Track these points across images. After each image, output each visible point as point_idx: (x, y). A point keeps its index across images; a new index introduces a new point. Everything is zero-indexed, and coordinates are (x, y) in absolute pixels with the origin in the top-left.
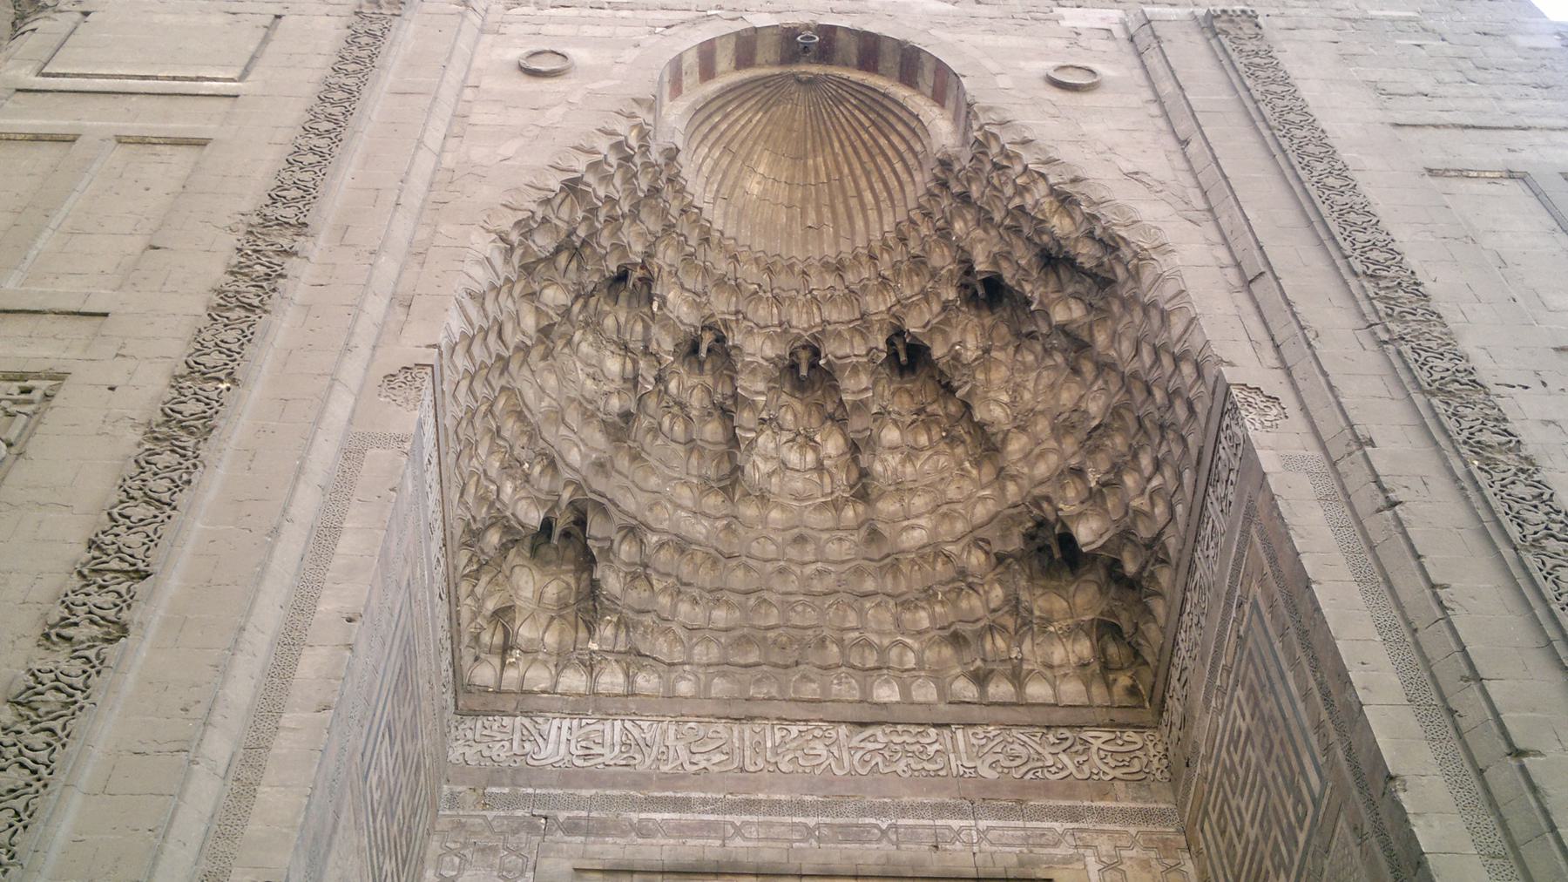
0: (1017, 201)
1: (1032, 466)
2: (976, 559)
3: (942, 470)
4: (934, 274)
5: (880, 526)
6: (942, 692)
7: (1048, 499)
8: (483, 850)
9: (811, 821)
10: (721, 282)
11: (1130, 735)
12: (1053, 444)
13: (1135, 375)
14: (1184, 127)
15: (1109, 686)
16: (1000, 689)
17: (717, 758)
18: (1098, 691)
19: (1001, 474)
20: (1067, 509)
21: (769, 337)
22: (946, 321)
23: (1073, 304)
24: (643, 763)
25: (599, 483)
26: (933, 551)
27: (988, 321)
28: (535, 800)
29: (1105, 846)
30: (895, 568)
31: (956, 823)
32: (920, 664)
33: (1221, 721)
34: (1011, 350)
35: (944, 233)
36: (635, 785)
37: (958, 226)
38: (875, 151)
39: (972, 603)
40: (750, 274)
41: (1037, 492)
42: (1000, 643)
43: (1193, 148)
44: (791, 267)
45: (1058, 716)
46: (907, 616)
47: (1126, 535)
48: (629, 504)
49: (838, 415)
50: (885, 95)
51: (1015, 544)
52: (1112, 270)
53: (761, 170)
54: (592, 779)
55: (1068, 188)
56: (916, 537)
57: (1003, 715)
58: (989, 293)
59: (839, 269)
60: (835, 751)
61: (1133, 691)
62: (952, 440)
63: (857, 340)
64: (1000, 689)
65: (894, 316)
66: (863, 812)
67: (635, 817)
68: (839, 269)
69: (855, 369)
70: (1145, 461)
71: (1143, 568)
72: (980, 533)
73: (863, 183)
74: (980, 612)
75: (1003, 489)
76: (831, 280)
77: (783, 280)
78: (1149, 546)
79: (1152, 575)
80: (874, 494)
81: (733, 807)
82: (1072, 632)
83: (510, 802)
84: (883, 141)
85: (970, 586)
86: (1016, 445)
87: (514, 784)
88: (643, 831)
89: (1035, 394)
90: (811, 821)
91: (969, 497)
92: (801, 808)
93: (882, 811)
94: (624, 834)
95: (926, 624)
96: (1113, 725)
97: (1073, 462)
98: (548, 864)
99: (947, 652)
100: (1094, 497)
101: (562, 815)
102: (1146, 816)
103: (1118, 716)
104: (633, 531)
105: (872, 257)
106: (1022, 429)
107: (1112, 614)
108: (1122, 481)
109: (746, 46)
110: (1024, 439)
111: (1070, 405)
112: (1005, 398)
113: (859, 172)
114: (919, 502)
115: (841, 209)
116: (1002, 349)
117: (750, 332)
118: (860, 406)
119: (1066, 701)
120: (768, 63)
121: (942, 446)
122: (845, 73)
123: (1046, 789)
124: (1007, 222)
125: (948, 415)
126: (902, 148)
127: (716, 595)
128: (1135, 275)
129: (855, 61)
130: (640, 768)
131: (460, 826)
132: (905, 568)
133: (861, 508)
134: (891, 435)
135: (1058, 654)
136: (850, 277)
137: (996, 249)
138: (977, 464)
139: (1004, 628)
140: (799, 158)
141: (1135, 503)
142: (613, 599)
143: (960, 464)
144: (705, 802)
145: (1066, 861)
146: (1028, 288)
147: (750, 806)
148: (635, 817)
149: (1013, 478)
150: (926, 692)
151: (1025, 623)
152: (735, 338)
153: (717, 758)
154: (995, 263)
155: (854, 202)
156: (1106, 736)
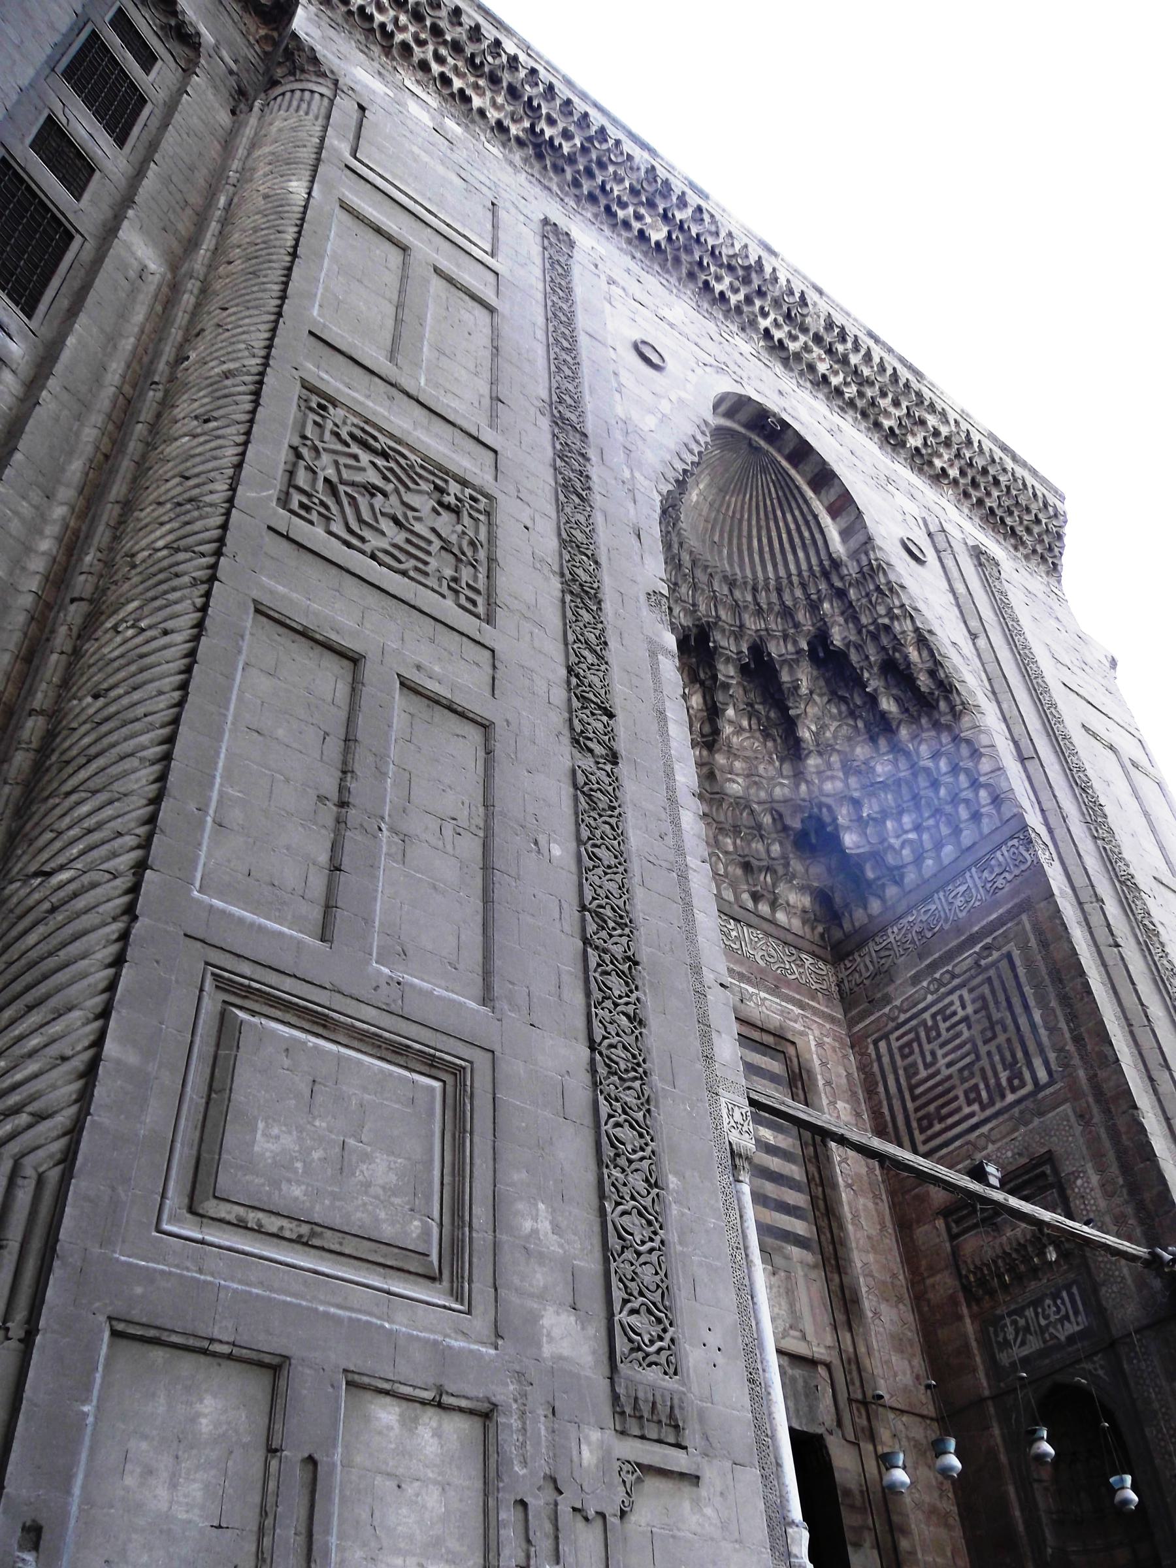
0: (886, 621)
1: (822, 781)
2: (767, 820)
3: (756, 751)
4: (797, 625)
5: (717, 773)
7: (829, 808)
11: (821, 964)
12: (841, 774)
13: (927, 770)
14: (974, 624)
15: (813, 929)
16: (764, 908)
18: (807, 929)
19: (798, 776)
20: (841, 820)
21: (684, 609)
22: (797, 661)
23: (892, 701)
26: (742, 804)
27: (815, 673)
29: (817, 1033)
30: (720, 802)
31: (751, 990)
33: (930, 998)
34: (825, 699)
35: (814, 607)
37: (826, 605)
38: (771, 516)
39: (757, 846)
41: (824, 799)
43: (982, 642)
44: (706, 567)
45: (790, 938)
46: (720, 838)
47: (876, 856)
49: (708, 683)
50: (797, 487)
51: (796, 824)
52: (938, 701)
53: (701, 486)
55: (927, 635)
56: (735, 788)
57: (765, 925)
58: (827, 658)
59: (732, 584)
61: (822, 935)
62: (766, 735)
63: (732, 640)
65: (760, 637)
69: (728, 660)
70: (907, 820)
71: (878, 878)
72: (775, 805)
75: (797, 786)
76: (726, 591)
78: (891, 869)
79: (883, 886)
80: (717, 746)
82: (802, 889)
84: (779, 513)
85: (762, 837)
86: (812, 762)
89: (835, 737)
91: (773, 778)
95: (731, 848)
96: (813, 954)
97: (856, 794)
99: (739, 872)
100: (861, 823)
102: (832, 1020)
103: (818, 950)
105: (755, 589)
106: (820, 754)
107: (832, 888)
108: (884, 823)
110: (819, 761)
111: (862, 758)
112: (813, 728)
113: (754, 522)
114: (738, 765)
116: (821, 695)
118: (726, 686)
120: (739, 423)
121: (758, 734)
122: (779, 458)
123: (788, 984)
124: (872, 628)
125: (768, 718)
126: (792, 526)
128: (956, 715)
129: (787, 451)
132: (725, 806)
133: (705, 753)
134: (730, 712)
137: (853, 638)
138: (782, 760)
139: (775, 872)
140: (723, 491)
141: (892, 841)
143: (770, 755)
145: (802, 1034)
146: (866, 675)
149: (807, 782)
154: (848, 645)
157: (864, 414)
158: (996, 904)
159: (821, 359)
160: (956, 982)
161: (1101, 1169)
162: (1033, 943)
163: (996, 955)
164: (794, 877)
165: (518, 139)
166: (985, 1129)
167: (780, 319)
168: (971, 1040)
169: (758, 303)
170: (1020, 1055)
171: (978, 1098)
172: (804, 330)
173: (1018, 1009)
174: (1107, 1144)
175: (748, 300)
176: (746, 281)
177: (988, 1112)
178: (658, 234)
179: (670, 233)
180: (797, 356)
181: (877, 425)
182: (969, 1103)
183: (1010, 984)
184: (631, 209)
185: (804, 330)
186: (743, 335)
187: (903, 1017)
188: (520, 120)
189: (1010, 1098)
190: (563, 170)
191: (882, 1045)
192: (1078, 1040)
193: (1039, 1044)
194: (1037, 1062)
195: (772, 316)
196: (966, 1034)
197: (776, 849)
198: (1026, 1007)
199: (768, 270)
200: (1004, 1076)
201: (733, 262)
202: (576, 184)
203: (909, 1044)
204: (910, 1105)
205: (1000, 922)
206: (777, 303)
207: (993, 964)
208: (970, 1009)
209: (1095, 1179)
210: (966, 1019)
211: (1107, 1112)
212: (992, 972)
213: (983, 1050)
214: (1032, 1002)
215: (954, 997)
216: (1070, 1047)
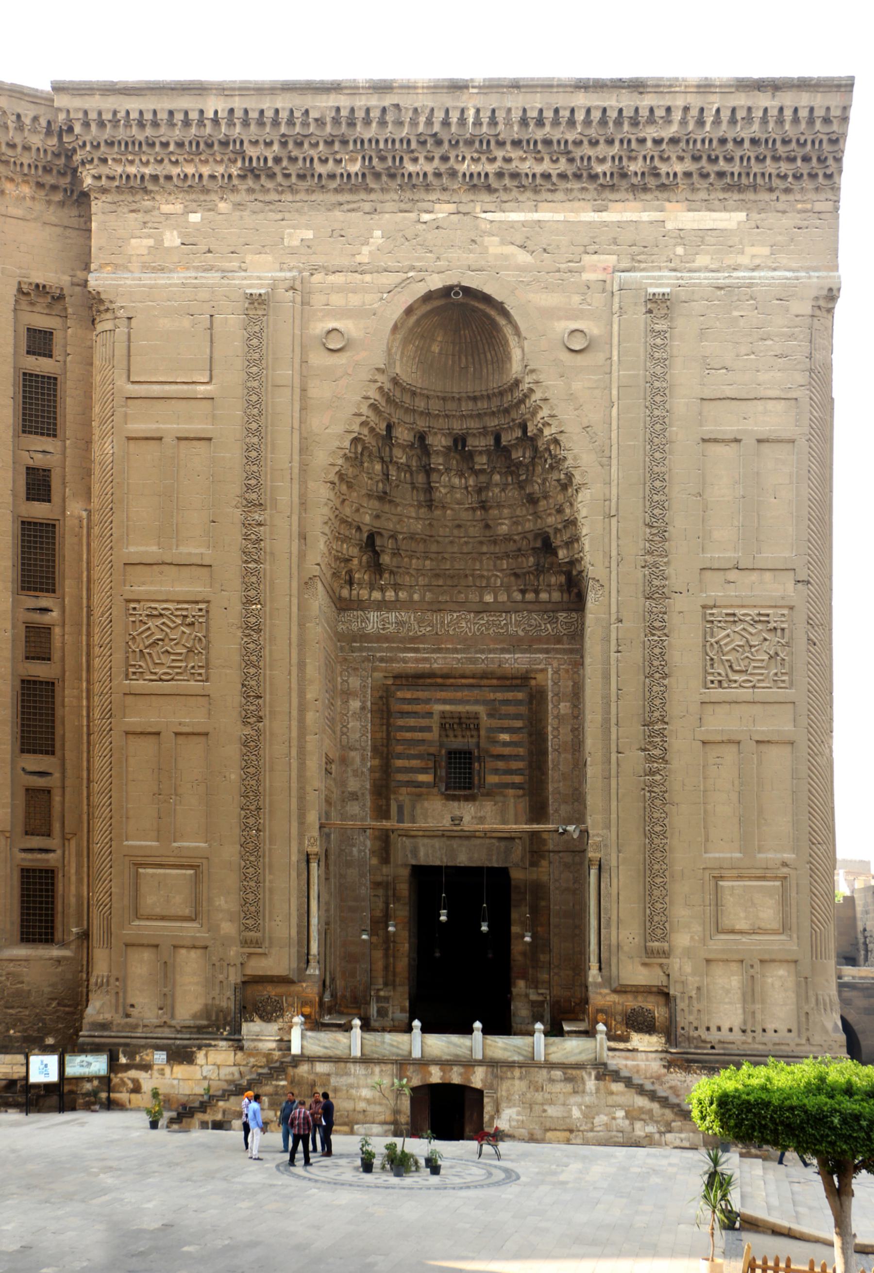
6: (509, 597)
8: (355, 669)
9: (459, 656)
10: (422, 413)
11: (574, 615)
15: (570, 593)
16: (530, 596)
17: (428, 629)
18: (566, 596)
24: (403, 632)
25: (377, 524)
26: (508, 538)
28: (369, 649)
32: (502, 585)
36: (401, 642)
40: (435, 406)
42: (532, 577)
45: (550, 606)
48: (391, 526)
54: (387, 639)
56: (504, 529)
57: (530, 607)
60: (467, 624)
64: (530, 596)
66: (476, 652)
67: (402, 655)
68: (475, 399)
69: (481, 453)
73: (486, 348)
74: (525, 565)
76: (471, 405)
77: (450, 405)
81: (434, 651)
83: (361, 649)
87: (361, 642)
88: (404, 661)
90: (459, 656)
92: (456, 651)
93: (482, 652)
94: (399, 662)
98: (375, 674)
101: (378, 655)
104: (391, 537)
109: (429, 297)
115: (476, 358)
117: (436, 434)
118: (482, 471)
119: (553, 600)
127: (426, 556)
130: (402, 635)
131: (346, 660)
135: (553, 580)
136: (479, 404)
142: (388, 566)
144: (424, 649)
147: (439, 650)
148: (402, 655)
150: (503, 597)
151: (539, 570)
152: (430, 440)
153: (428, 629)
155: (482, 356)
156: (565, 615)
157: (578, 176)
159: (523, 160)
164: (551, 568)
165: (239, 176)
167: (476, 155)
169: (452, 155)
172: (501, 144)
175: (445, 159)
176: (439, 143)
178: (355, 168)
179: (364, 158)
180: (500, 175)
184: (331, 162)
185: (501, 144)
186: (445, 196)
188: (235, 161)
190: (275, 174)
195: (468, 157)
197: (531, 559)
199: (454, 117)
201: (422, 139)
202: (287, 176)
206: (469, 143)
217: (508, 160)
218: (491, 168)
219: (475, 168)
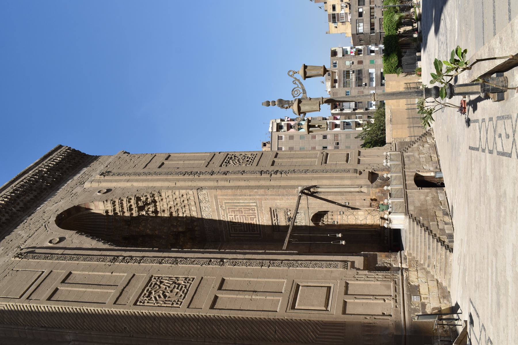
0: (129, 205)
157: (42, 192)
158: (212, 202)
160: (225, 215)
161: (277, 199)
162: (225, 197)
163: (224, 205)
166: (260, 219)
168: (240, 216)
170: (248, 207)
171: (253, 218)
173: (238, 204)
174: (273, 197)
175: (7, 213)
177: (257, 217)
180: (25, 204)
181: (45, 189)
182: (253, 220)
183: (232, 204)
187: (228, 229)
189: (256, 212)
191: (232, 235)
192: (250, 195)
193: (248, 203)
194: (251, 204)
196: (238, 217)
198: (239, 203)
200: (251, 212)
203: (234, 229)
204: (248, 233)
205: (217, 202)
207: (226, 206)
208: (233, 214)
209: (278, 201)
210: (235, 216)
211: (267, 195)
212: (227, 207)
213: (243, 214)
214: (238, 201)
215: (229, 217)
216: (251, 197)
217: (22, 201)
218: (21, 205)
219: (18, 207)
